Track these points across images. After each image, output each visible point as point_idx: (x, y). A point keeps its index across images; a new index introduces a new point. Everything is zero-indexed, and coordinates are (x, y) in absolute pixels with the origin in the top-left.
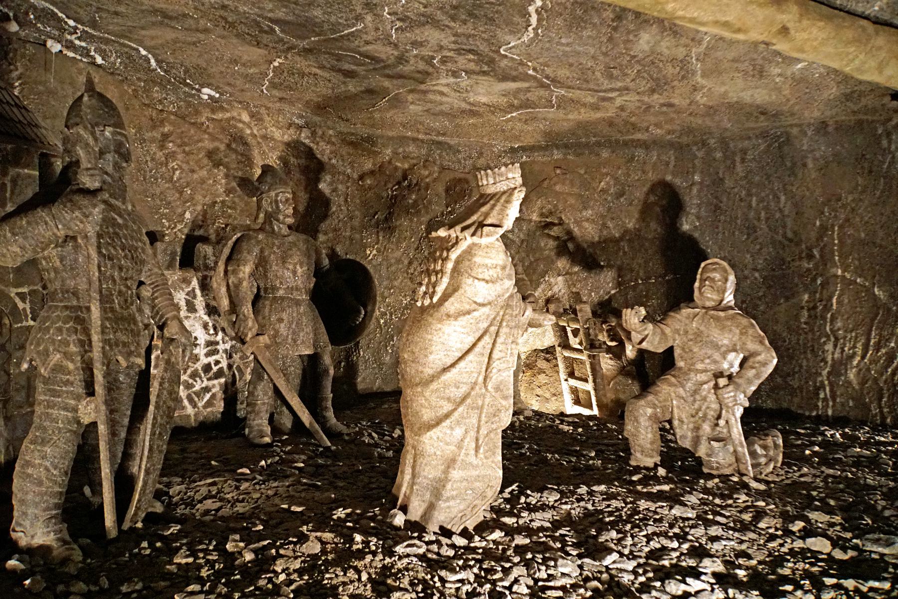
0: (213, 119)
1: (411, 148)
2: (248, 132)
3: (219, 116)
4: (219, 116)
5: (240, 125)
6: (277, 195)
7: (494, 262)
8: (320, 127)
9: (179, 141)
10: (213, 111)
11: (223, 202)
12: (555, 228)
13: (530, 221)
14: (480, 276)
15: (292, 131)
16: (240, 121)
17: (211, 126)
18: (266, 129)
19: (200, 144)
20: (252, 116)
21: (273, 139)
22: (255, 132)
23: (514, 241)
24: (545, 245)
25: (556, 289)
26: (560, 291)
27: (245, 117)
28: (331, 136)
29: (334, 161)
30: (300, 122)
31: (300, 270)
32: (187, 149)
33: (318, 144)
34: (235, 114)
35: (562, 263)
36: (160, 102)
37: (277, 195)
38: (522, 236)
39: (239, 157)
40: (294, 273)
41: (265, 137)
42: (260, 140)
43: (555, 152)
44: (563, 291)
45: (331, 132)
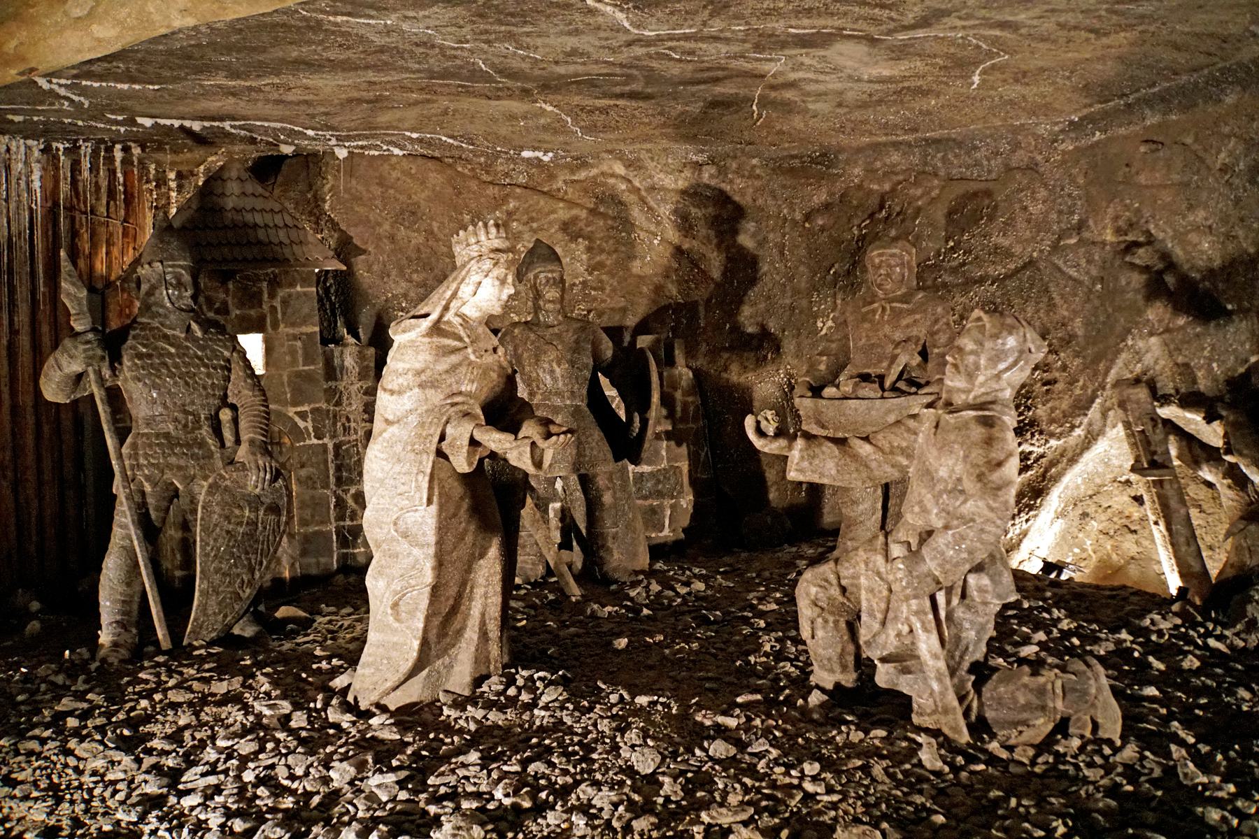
0: (576, 181)
1: (895, 157)
2: (623, 187)
3: (582, 175)
4: (582, 175)
5: (612, 181)
6: (536, 277)
7: (407, 366)
8: (735, 157)
9: (525, 218)
10: (573, 172)
11: (584, 283)
12: (1141, 251)
13: (1104, 243)
14: (390, 387)
15: (687, 173)
16: (613, 175)
17: (570, 190)
18: (651, 177)
19: (552, 217)
20: (627, 167)
21: (663, 189)
22: (637, 184)
23: (1080, 283)
24: (1128, 283)
25: (1148, 359)
26: (1156, 363)
27: (619, 169)
28: (755, 166)
29: (760, 202)
30: (700, 158)
31: (558, 370)
32: (535, 225)
33: (731, 182)
34: (605, 168)
35: (1156, 313)
36: (507, 175)
37: (536, 277)
38: (1094, 272)
39: (610, 222)
40: (552, 372)
41: (652, 189)
42: (643, 193)
43: (1147, 112)
44: (1162, 362)
45: (755, 161)
